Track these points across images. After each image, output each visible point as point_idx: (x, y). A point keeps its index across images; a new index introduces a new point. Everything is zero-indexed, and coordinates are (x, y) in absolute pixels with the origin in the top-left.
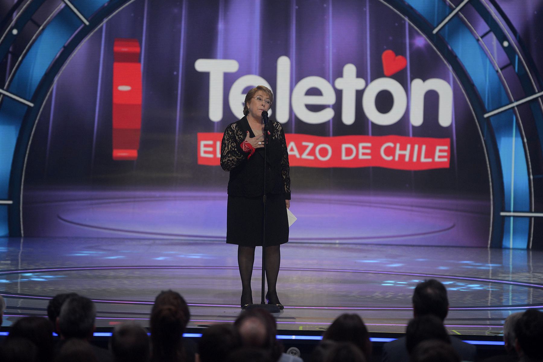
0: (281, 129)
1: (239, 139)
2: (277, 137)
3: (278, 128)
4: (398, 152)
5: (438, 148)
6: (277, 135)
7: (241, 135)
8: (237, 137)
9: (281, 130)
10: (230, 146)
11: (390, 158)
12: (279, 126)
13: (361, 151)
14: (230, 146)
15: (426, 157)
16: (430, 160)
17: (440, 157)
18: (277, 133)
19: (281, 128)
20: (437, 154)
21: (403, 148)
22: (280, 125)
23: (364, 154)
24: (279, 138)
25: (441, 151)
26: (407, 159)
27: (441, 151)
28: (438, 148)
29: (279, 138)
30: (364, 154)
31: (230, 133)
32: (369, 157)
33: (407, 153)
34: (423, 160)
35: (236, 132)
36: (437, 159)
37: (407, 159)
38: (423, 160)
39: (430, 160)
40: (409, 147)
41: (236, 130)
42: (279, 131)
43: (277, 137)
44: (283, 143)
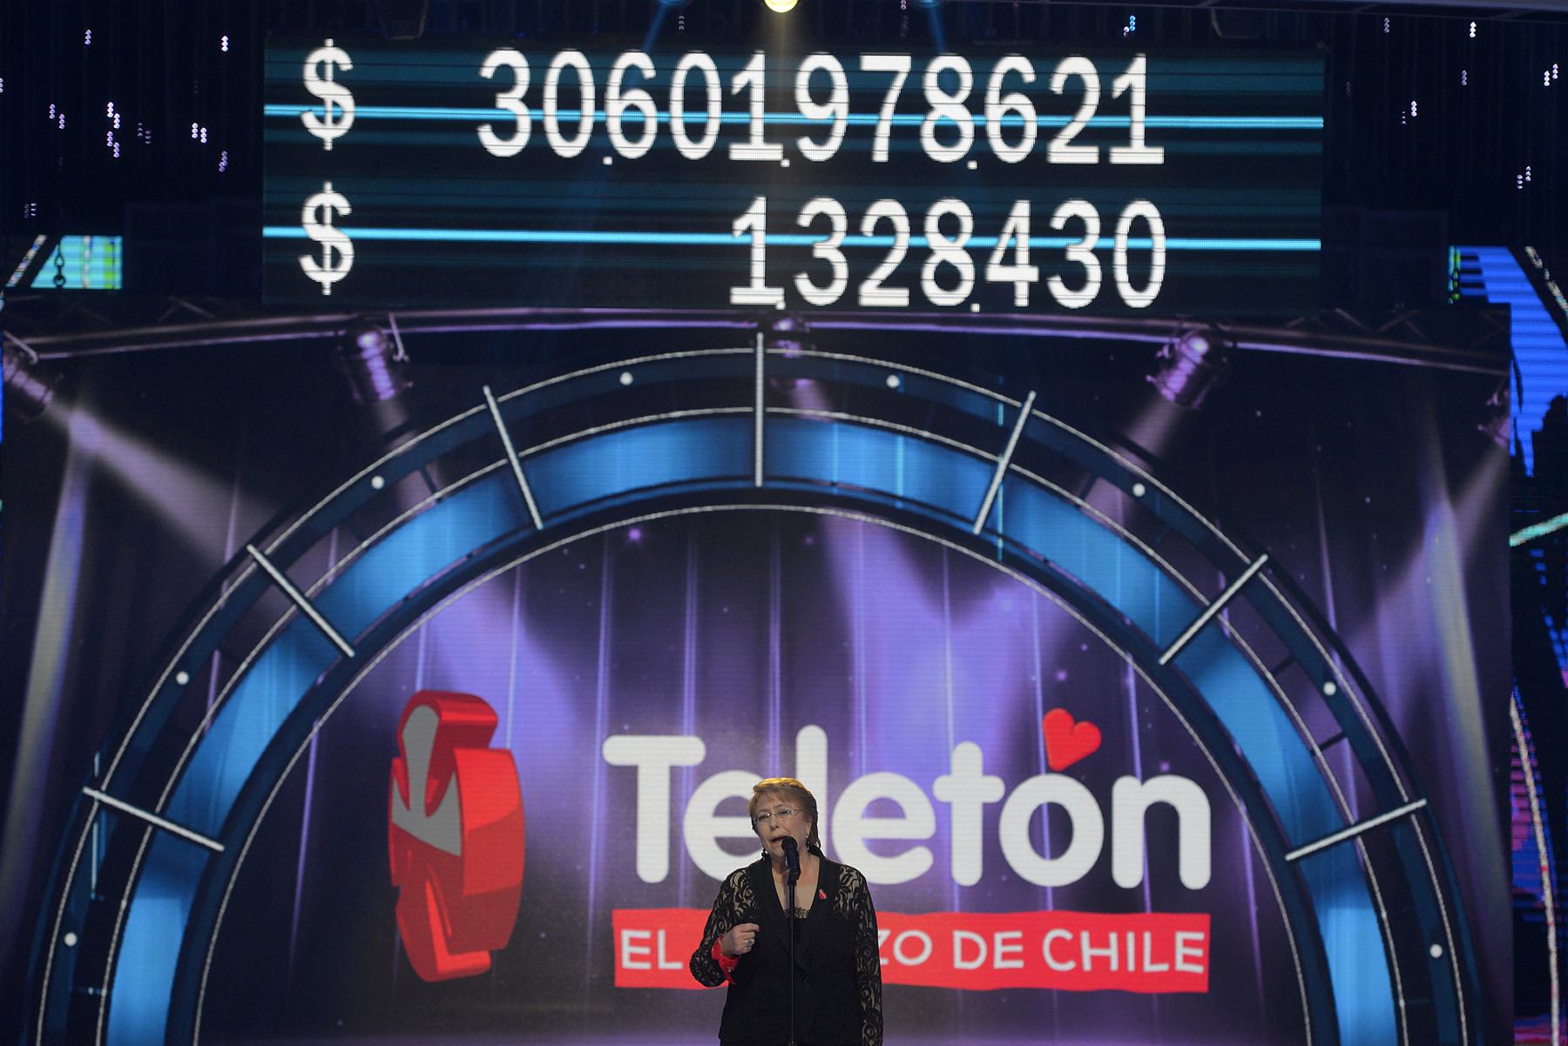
0: (858, 885)
1: (743, 908)
2: (841, 906)
3: (849, 883)
4: (1088, 952)
6: (845, 900)
7: (747, 898)
8: (737, 904)
9: (856, 888)
10: (715, 928)
11: (1069, 965)
12: (851, 879)
13: (999, 949)
14: (715, 928)
15: (1154, 961)
18: (844, 896)
19: (856, 884)
21: (1099, 941)
22: (855, 877)
23: (1006, 956)
24: (848, 908)
26: (1114, 966)
29: (848, 908)
30: (1006, 956)
31: (725, 896)
32: (1019, 964)
33: (1112, 952)
35: (738, 894)
37: (1114, 966)
40: (1113, 937)
41: (739, 887)
42: (850, 891)
43: (841, 906)
44: (860, 921)
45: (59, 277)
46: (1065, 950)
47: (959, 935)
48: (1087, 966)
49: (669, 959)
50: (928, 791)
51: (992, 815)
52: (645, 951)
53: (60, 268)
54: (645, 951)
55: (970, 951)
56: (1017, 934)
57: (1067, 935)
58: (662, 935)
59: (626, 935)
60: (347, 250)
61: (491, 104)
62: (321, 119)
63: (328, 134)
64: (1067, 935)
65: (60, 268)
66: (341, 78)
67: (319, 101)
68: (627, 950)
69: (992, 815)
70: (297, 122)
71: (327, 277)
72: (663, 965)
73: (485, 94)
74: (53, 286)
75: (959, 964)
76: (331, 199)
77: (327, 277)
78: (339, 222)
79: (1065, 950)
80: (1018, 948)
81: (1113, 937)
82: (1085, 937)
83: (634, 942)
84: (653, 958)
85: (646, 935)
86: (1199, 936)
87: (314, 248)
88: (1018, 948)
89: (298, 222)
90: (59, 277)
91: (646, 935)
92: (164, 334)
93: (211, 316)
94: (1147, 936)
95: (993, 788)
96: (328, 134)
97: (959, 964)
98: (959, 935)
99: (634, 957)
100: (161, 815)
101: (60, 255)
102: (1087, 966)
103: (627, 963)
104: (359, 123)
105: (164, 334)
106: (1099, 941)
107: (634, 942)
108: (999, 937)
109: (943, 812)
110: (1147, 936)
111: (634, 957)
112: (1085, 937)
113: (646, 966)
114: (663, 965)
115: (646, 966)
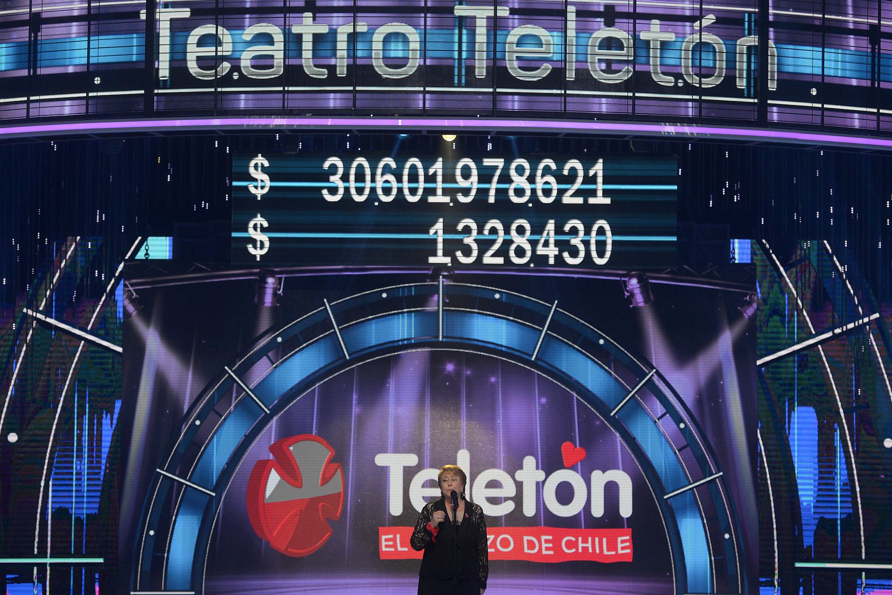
4: (581, 545)
5: (620, 539)
11: (574, 550)
16: (613, 553)
17: (623, 548)
20: (620, 545)
21: (585, 541)
25: (623, 542)
27: (623, 542)
28: (620, 539)
33: (589, 545)
34: (605, 552)
36: (620, 552)
38: (605, 552)
39: (613, 553)
40: (590, 539)
45: (147, 254)
46: (569, 545)
47: (526, 538)
48: (580, 550)
49: (401, 546)
50: (513, 477)
51: (540, 486)
52: (391, 543)
53: (147, 250)
54: (391, 543)
55: (531, 545)
56: (550, 538)
57: (574, 539)
58: (398, 536)
59: (384, 537)
60: (267, 244)
61: (328, 181)
62: (256, 187)
63: (259, 193)
64: (574, 539)
65: (147, 250)
66: (264, 170)
67: (256, 180)
68: (384, 543)
69: (540, 486)
70: (246, 188)
71: (258, 253)
72: (399, 549)
73: (325, 176)
74: (144, 258)
75: (526, 551)
76: (260, 220)
77: (258, 253)
78: (263, 230)
79: (569, 545)
80: (550, 545)
81: (590, 539)
82: (580, 539)
83: (386, 540)
84: (395, 546)
85: (391, 536)
86: (627, 538)
87: (253, 241)
88: (550, 545)
89: (246, 230)
90: (147, 254)
91: (391, 536)
92: (191, 278)
93: (210, 270)
94: (605, 540)
95: (541, 475)
96: (259, 193)
97: (526, 551)
98: (526, 538)
99: (387, 546)
100: (189, 481)
101: (147, 245)
102: (580, 550)
103: (384, 549)
104: (272, 188)
105: (191, 278)
106: (585, 541)
107: (386, 540)
108: (543, 538)
109: (519, 486)
110: (605, 540)
111: (387, 546)
112: (580, 539)
113: (393, 549)
114: (399, 549)
115: (393, 549)
